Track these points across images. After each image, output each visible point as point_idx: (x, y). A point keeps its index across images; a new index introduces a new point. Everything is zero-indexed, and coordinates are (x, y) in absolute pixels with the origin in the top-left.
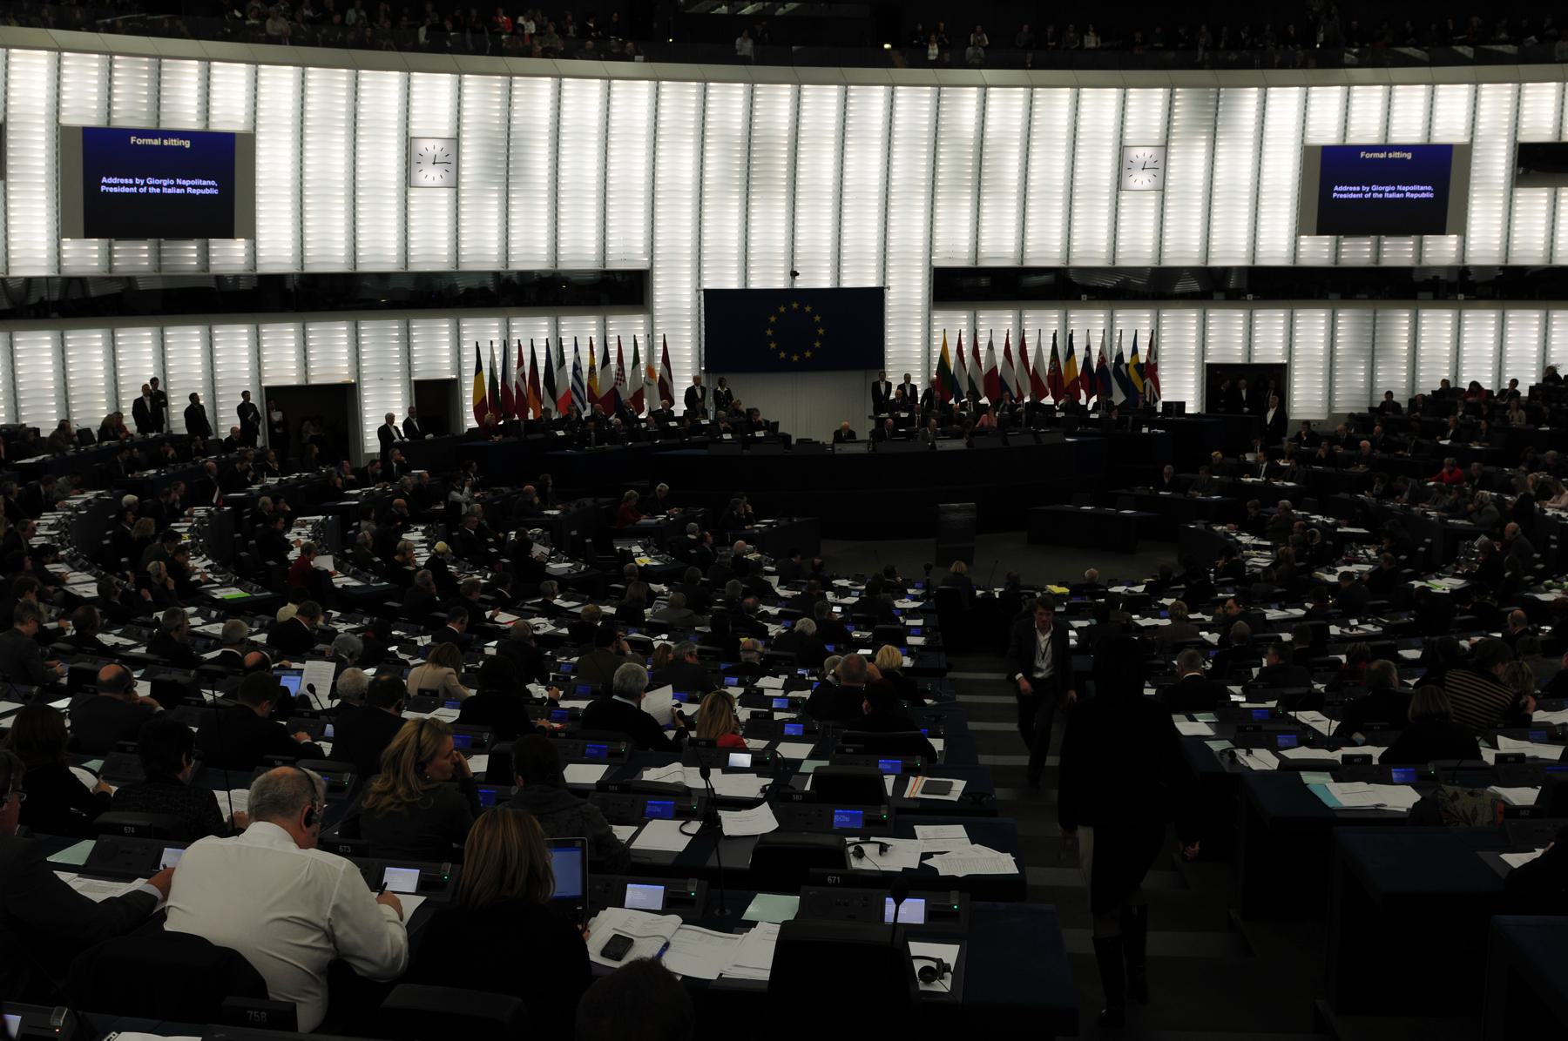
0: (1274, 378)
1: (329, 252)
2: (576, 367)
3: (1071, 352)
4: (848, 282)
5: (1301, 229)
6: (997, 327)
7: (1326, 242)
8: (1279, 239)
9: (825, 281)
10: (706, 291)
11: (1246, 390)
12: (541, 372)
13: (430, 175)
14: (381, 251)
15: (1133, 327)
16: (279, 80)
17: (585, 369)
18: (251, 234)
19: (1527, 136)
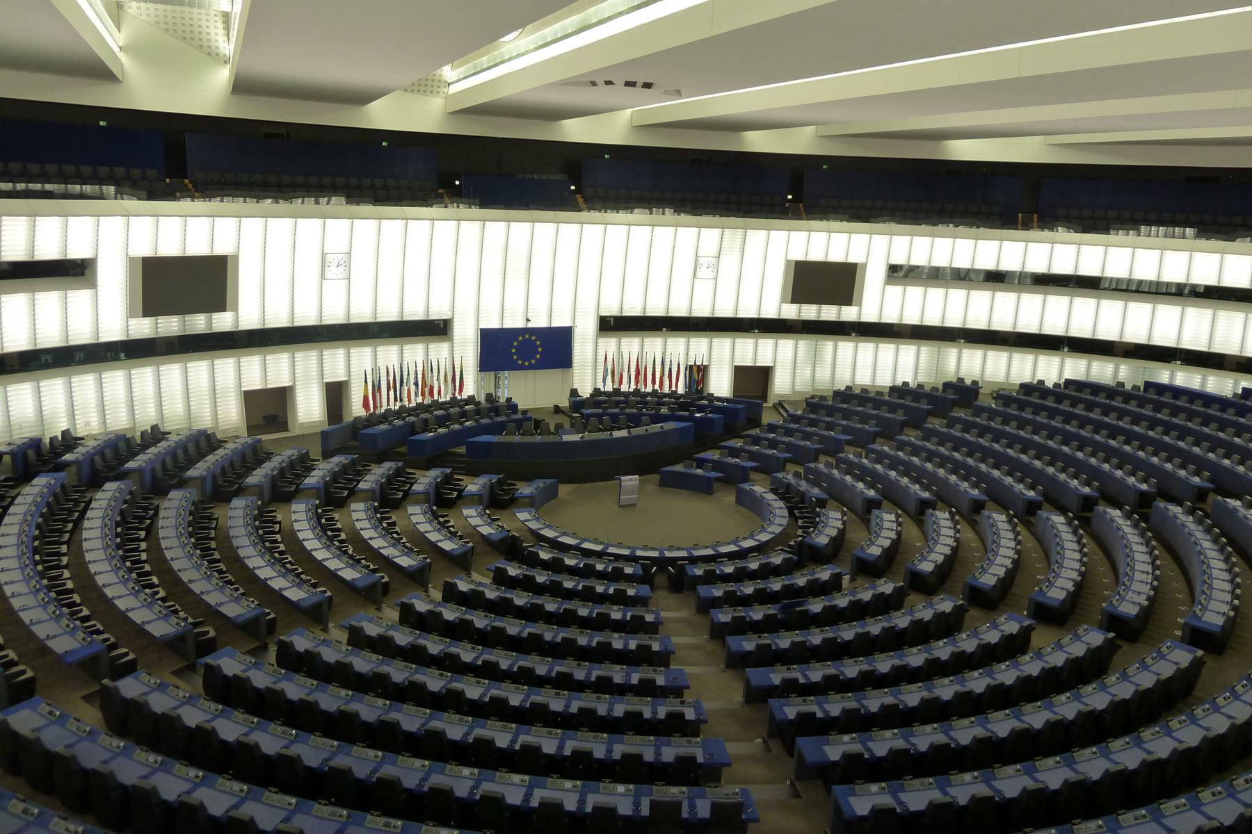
0: (764, 374)
1: (278, 318)
5: (783, 301)
6: (631, 345)
7: (795, 306)
8: (774, 306)
10: (482, 330)
11: (754, 380)
13: (332, 272)
14: (307, 317)
15: (698, 348)
16: (252, 226)
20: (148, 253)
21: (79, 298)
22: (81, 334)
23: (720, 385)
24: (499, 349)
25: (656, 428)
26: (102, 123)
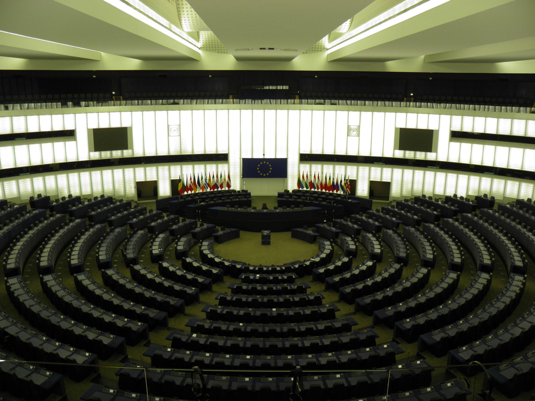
0: (387, 186)
1: (150, 152)
2: (206, 179)
3: (330, 178)
4: (278, 157)
5: (395, 149)
7: (402, 152)
8: (390, 150)
9: (272, 156)
10: (243, 159)
11: (380, 189)
12: (197, 181)
14: (162, 152)
16: (137, 115)
17: (208, 179)
18: (132, 148)
20: (96, 127)
21: (70, 144)
22: (72, 158)
24: (253, 168)
25: (305, 209)
26: (94, 77)
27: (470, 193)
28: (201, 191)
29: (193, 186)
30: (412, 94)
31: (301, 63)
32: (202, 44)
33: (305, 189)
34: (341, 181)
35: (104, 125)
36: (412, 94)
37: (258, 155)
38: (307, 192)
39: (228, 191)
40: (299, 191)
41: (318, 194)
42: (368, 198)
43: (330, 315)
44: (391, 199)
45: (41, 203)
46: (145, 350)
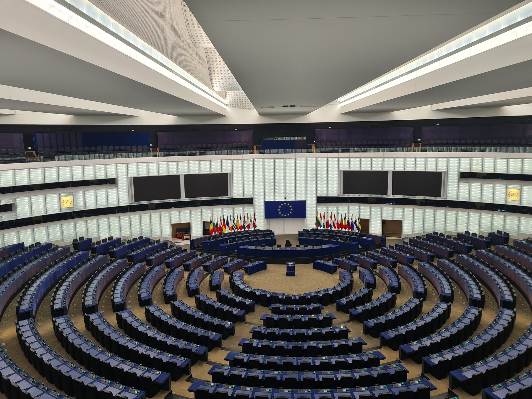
0: (399, 224)
9: (293, 199)
11: (392, 227)
17: (236, 220)
19: (463, 170)
21: (112, 191)
22: (113, 203)
23: (376, 229)
27: (483, 230)
28: (230, 231)
29: (223, 228)
30: (419, 140)
31: (318, 116)
32: (229, 101)
33: (322, 228)
34: (356, 221)
35: (143, 173)
36: (419, 140)
37: (280, 198)
38: (324, 230)
39: (254, 231)
40: (317, 230)
41: (335, 233)
42: (381, 236)
43: (357, 348)
44: (403, 236)
45: (83, 244)
46: (189, 384)
